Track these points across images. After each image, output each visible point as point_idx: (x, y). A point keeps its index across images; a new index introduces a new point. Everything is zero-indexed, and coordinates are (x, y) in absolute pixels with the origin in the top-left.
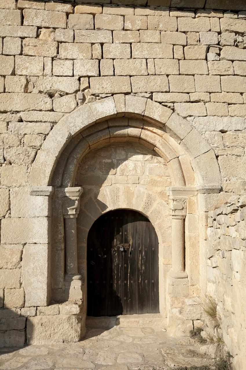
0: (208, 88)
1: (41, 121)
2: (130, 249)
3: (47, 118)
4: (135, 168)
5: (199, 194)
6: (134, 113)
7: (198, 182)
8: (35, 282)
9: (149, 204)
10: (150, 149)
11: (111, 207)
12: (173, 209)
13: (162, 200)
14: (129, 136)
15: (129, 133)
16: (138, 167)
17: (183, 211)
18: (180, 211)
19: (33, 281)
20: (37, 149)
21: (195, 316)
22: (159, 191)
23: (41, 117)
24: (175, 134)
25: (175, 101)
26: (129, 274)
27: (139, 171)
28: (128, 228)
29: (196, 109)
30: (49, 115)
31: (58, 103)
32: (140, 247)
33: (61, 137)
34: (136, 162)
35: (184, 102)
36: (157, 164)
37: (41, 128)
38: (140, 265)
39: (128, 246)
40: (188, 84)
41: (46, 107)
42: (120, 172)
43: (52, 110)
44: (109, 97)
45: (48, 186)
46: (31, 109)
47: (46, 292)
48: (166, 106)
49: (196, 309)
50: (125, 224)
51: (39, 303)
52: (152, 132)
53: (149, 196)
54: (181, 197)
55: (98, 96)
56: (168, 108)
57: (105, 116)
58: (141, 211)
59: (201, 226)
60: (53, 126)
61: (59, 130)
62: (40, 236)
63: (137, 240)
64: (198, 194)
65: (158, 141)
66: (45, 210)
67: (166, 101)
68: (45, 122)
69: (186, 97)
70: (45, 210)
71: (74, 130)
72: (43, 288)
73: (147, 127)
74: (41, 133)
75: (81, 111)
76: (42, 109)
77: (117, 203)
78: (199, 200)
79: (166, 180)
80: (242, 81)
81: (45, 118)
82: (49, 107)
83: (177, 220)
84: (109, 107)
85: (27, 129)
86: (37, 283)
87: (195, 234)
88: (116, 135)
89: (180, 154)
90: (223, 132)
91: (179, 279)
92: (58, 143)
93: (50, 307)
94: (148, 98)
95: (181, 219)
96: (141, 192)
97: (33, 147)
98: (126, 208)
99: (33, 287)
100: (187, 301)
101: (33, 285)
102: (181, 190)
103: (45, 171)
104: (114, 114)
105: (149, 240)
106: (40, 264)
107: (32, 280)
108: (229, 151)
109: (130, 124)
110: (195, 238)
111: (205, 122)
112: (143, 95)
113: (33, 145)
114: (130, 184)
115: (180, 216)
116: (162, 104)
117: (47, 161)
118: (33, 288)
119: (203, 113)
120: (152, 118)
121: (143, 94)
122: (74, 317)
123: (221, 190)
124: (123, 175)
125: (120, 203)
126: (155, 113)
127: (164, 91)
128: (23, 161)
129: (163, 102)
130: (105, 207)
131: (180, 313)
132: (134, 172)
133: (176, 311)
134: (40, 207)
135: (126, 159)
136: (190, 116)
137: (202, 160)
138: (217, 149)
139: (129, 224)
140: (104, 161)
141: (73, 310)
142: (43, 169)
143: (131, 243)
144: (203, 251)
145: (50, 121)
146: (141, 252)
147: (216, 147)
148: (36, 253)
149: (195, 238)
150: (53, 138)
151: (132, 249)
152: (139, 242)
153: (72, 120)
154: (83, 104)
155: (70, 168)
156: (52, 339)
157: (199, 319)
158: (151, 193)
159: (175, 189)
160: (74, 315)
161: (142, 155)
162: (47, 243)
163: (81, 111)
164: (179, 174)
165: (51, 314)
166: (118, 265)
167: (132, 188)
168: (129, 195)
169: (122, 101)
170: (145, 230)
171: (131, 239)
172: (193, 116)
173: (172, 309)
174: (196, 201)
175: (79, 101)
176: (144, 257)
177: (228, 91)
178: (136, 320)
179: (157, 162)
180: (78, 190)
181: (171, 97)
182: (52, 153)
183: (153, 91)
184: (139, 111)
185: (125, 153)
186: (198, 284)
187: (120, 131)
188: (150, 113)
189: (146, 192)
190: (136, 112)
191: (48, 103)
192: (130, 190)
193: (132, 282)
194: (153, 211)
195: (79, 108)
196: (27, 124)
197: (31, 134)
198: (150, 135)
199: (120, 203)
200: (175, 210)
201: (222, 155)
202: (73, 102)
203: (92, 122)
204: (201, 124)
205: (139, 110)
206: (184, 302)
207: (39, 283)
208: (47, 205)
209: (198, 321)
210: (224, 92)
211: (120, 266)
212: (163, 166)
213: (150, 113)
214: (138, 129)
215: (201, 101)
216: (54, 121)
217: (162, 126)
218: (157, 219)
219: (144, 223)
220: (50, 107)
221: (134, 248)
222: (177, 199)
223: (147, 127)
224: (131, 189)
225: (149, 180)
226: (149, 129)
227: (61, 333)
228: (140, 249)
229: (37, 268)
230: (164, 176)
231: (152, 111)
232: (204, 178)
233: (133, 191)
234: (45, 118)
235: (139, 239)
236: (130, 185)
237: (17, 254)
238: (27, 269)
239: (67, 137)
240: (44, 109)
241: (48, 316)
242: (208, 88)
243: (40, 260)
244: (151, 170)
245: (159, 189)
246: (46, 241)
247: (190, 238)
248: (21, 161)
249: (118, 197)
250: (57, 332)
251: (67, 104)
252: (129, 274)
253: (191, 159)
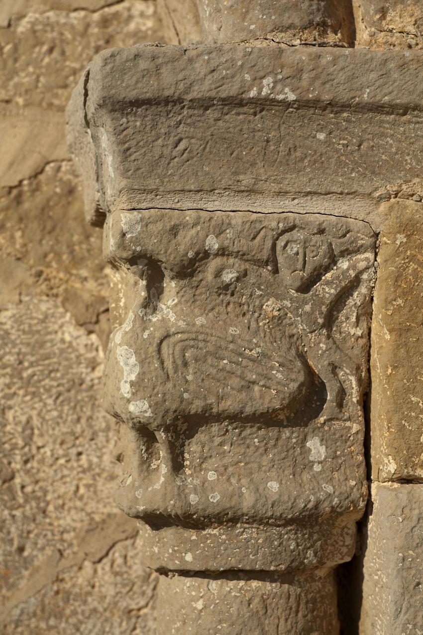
12: (139, 408)
17: (316, 448)
18: (256, 437)
54: (270, 208)
79: (105, 22)
83: (232, 586)
95: (286, 576)
102: (263, 104)
159: (168, 82)
222: (204, 255)
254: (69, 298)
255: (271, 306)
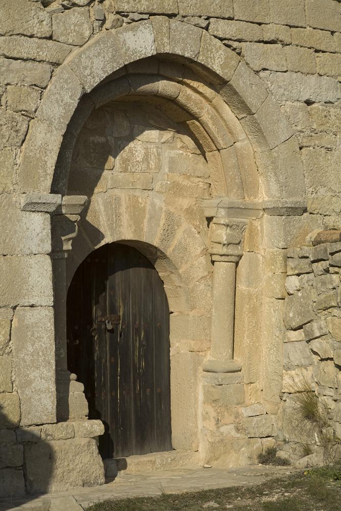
0: (289, 16)
1: (34, 60)
2: (120, 325)
3: (45, 53)
4: (146, 158)
5: (265, 215)
6: (183, 57)
7: (266, 192)
8: (36, 380)
9: (169, 232)
10: (178, 119)
11: (108, 239)
12: (225, 242)
13: (191, 226)
14: (156, 96)
15: (160, 90)
16: (151, 156)
17: (239, 248)
18: (235, 246)
19: (33, 378)
20: (29, 116)
21: (265, 431)
22: (185, 207)
23: (34, 51)
24: (243, 102)
25: (244, 38)
26: (119, 377)
27: (152, 164)
28: (117, 282)
29: (273, 56)
30: (48, 47)
31: (61, 24)
32: (137, 323)
33: (70, 95)
34: (151, 146)
35: (256, 42)
36: (181, 152)
37: (36, 74)
38: (136, 358)
39: (118, 320)
40: (260, 7)
41: (43, 30)
42: (120, 164)
43: (50, 38)
44: (146, 21)
45: (50, 193)
46: (15, 32)
47: (55, 396)
48: (229, 46)
49: (265, 419)
50: (110, 275)
51: (45, 418)
52: (195, 90)
53: (169, 215)
55: (127, 16)
56: (232, 50)
57: (138, 59)
58: (157, 246)
59: (270, 274)
60: (53, 70)
61: (66, 81)
62: (41, 292)
63: (132, 307)
64: (263, 215)
65: (207, 110)
66: (47, 241)
67: (230, 37)
68: (40, 61)
69: (255, 32)
70: (47, 241)
71: (92, 83)
72: (50, 390)
73: (188, 81)
74: (35, 85)
75: (102, 45)
76: (35, 33)
77: (117, 229)
78: (264, 227)
80: (333, 10)
81: (41, 53)
82: (45, 30)
83: (229, 263)
84: (144, 42)
85: (11, 74)
86: (40, 380)
87: (257, 289)
88: (139, 92)
89: (240, 139)
90: (309, 103)
91: (229, 374)
92: (65, 108)
93: (60, 424)
94: (202, 28)
96: (157, 208)
97: (23, 112)
98: (133, 239)
99: (34, 388)
100: (243, 411)
101: (33, 385)
103: (46, 162)
104: (152, 56)
105: (151, 308)
106: (43, 345)
107: (31, 377)
108: (317, 140)
109: (162, 73)
110: (257, 297)
111: (285, 83)
112: (196, 23)
113: (24, 109)
114: (137, 190)
115: (235, 256)
116: (230, 43)
117: (47, 140)
118: (33, 390)
119: (283, 66)
120: (211, 68)
121: (197, 20)
122: (94, 442)
123: (305, 210)
124: (125, 170)
125: (122, 229)
126: (214, 60)
127: (226, 17)
128: (7, 141)
129: (225, 39)
130: (99, 235)
131: (237, 430)
132: (144, 166)
133: (228, 430)
134: (38, 235)
135: (131, 138)
136: (264, 69)
137: (281, 155)
138: (302, 134)
139: (116, 273)
140: (92, 138)
141: (95, 428)
142: (43, 158)
143: (121, 314)
144: (273, 319)
145: (51, 61)
146: (138, 332)
147: (299, 131)
148: (36, 323)
149: (257, 297)
150: (57, 96)
151: (124, 327)
152: (134, 311)
153: (88, 61)
154: (101, 30)
155: (67, 156)
156: (66, 481)
157: (270, 435)
158: (172, 210)
159: (233, 206)
160: (94, 438)
161: (158, 131)
162: (52, 305)
163: (102, 45)
164: (237, 177)
165: (63, 438)
166: (100, 359)
167: (142, 197)
168: (137, 213)
169: (164, 31)
170: (144, 287)
171: (121, 305)
172: (268, 70)
173: (218, 428)
174: (259, 228)
175: (97, 24)
176: (144, 343)
177: (315, 26)
178: (150, 458)
179: (182, 147)
180: (83, 203)
181: (237, 30)
182: (57, 127)
183: (210, 15)
184: (191, 53)
185: (129, 124)
186: (258, 381)
187: (147, 85)
188: (207, 58)
189: (164, 209)
190: (186, 55)
191: (44, 23)
192: (139, 202)
193: (124, 392)
194: (176, 246)
195: (96, 36)
196: (10, 64)
197: (19, 85)
198: (194, 97)
199: (122, 229)
200: (229, 244)
201: (308, 147)
202: (86, 26)
203: (118, 68)
204: (280, 87)
205: (191, 51)
206: (238, 413)
207: (43, 380)
208: (50, 231)
209: (269, 439)
210: (310, 27)
211: (103, 361)
212: (190, 157)
213: (207, 58)
214: (173, 83)
215: (278, 42)
216: (57, 62)
217: (218, 83)
218: (182, 263)
219: (142, 271)
220: (48, 31)
221: (126, 323)
223: (188, 81)
224: (140, 201)
225: (169, 182)
226: (191, 84)
227: (78, 470)
228: (136, 326)
229: (38, 353)
230: (193, 176)
231: (210, 54)
232: (283, 186)
233: (143, 206)
234: (41, 53)
235: (135, 304)
236: (137, 193)
237: (5, 327)
238: (22, 356)
239: (79, 95)
240: (39, 35)
241: (57, 442)
242: (289, 16)
243: (43, 338)
244: (172, 161)
245: (185, 203)
246: (50, 301)
247: (250, 296)
248: (5, 140)
249: (118, 216)
250: (73, 469)
251: (76, 28)
252: (119, 377)
253: (259, 150)
254: (193, 225)
255: (237, 231)
